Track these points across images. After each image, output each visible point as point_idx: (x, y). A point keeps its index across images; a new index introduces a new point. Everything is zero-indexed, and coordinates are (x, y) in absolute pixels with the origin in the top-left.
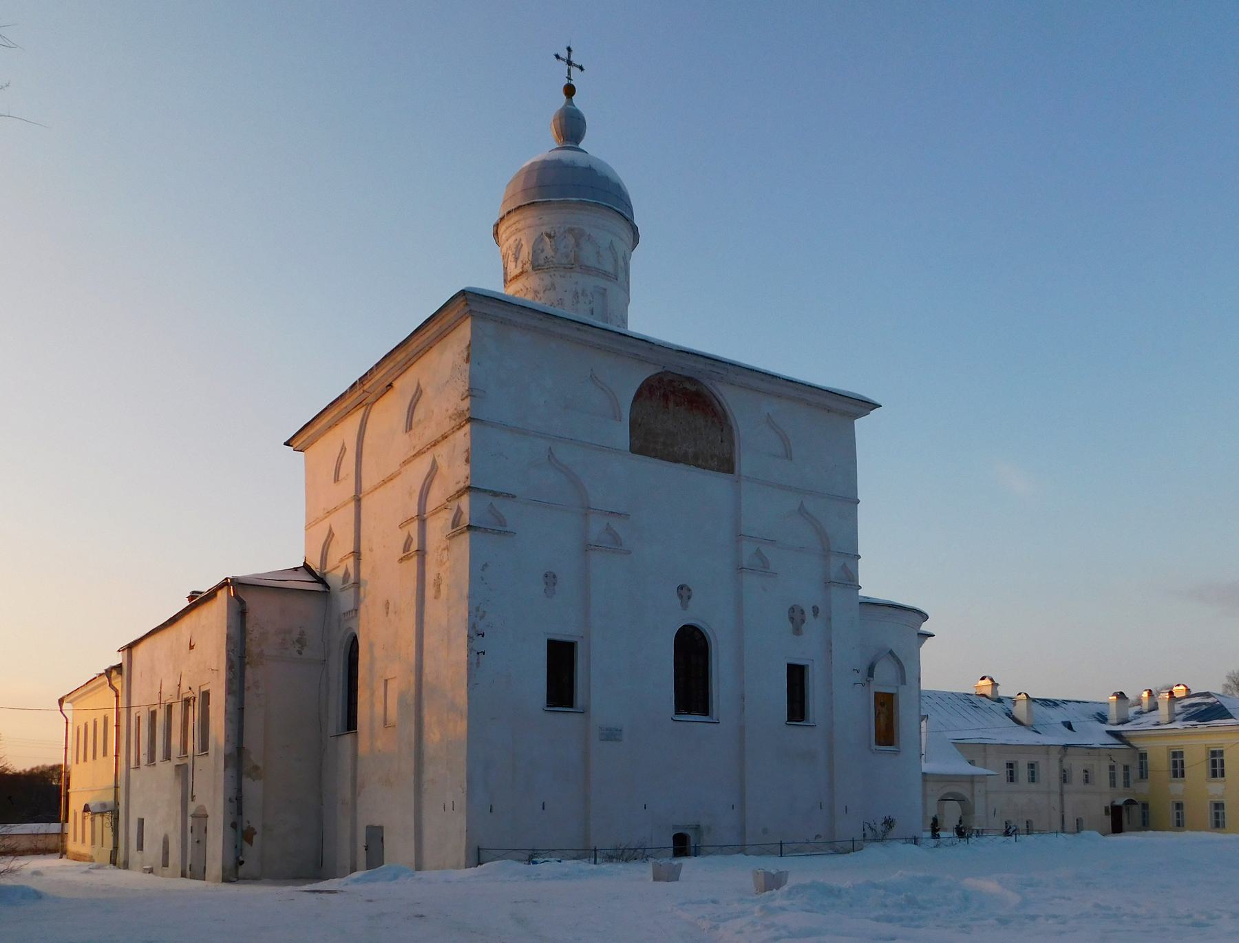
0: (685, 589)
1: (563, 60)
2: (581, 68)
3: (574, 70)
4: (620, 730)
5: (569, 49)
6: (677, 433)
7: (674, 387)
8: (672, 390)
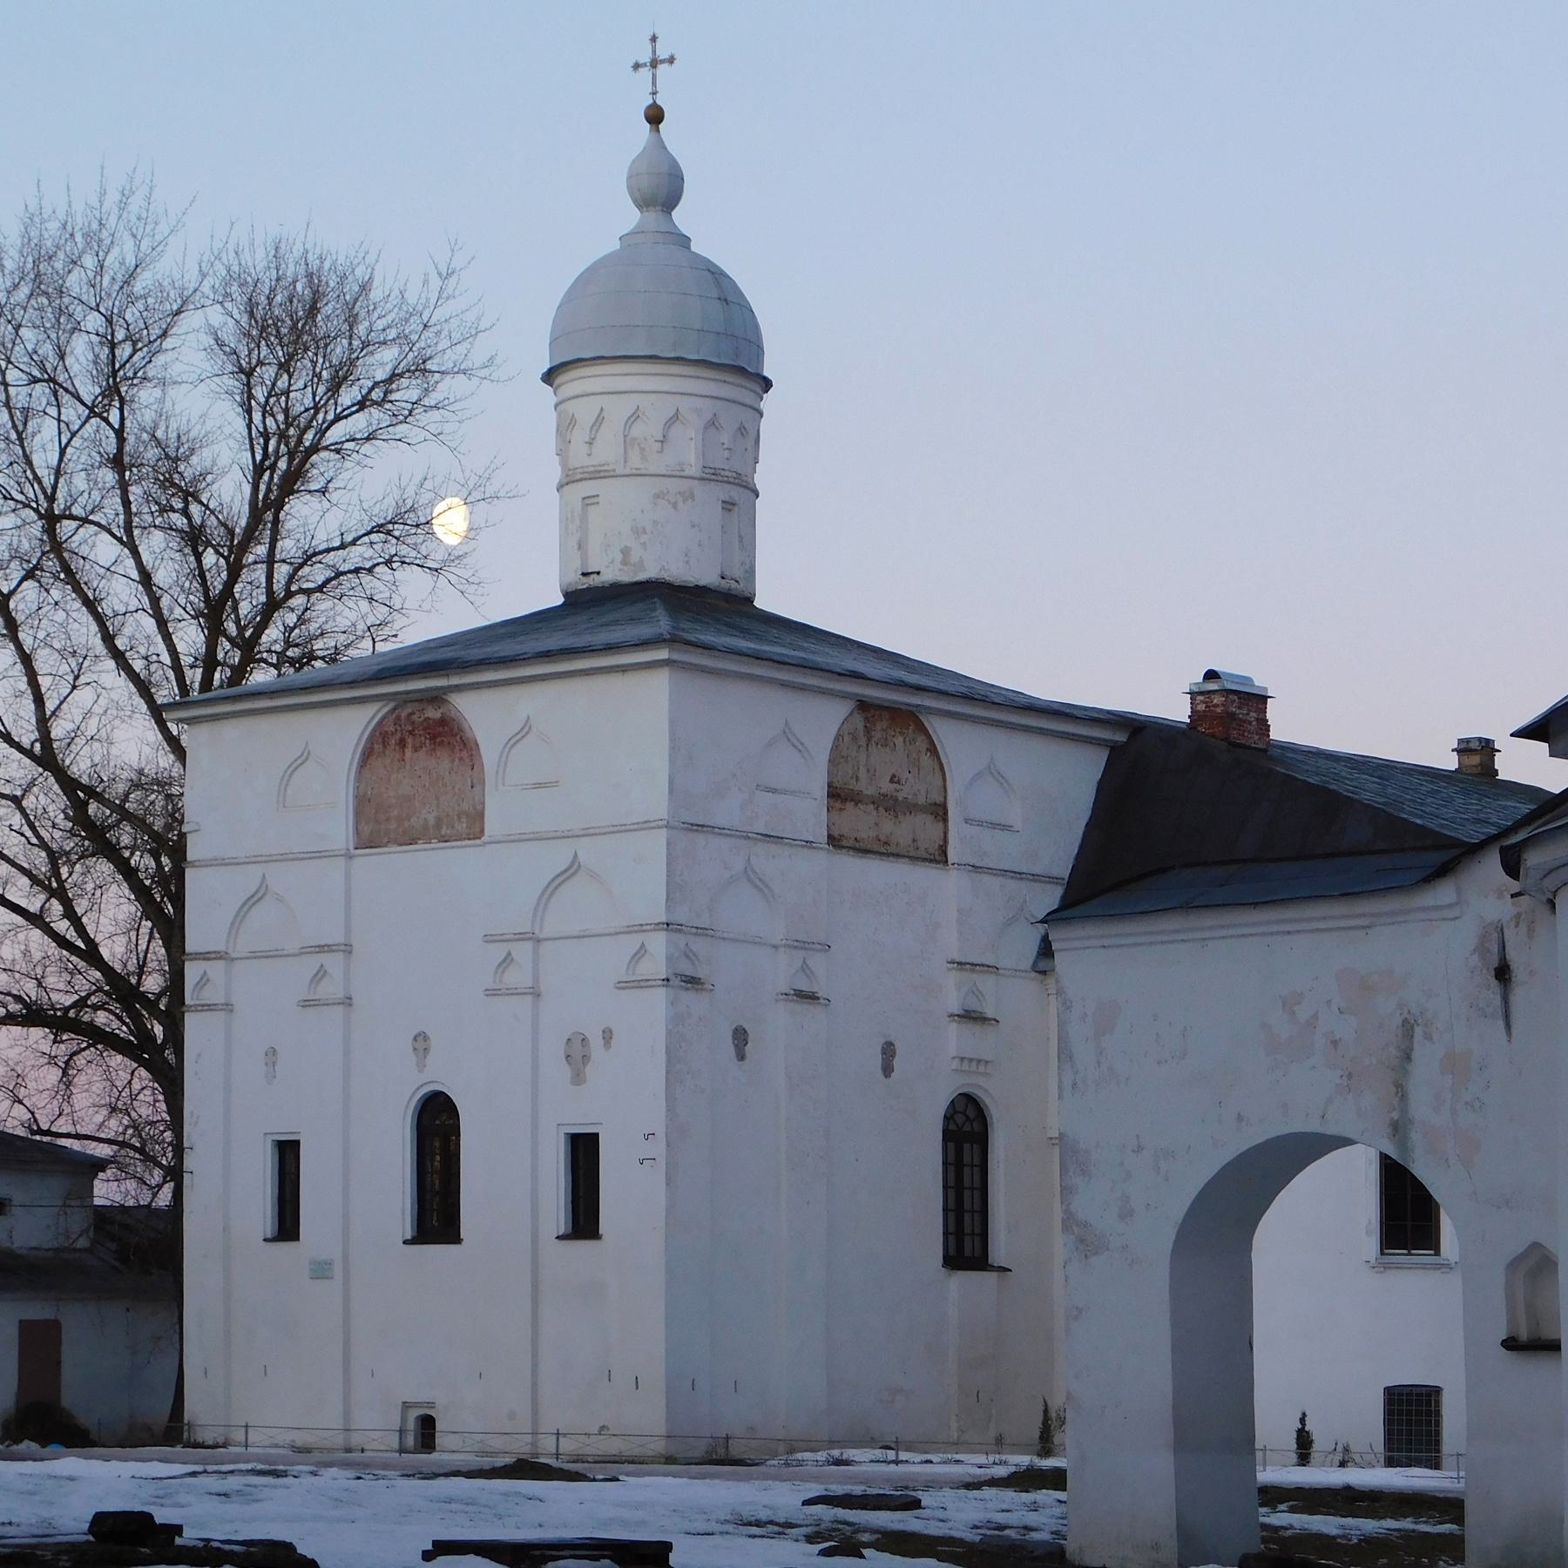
0: (420, 1039)
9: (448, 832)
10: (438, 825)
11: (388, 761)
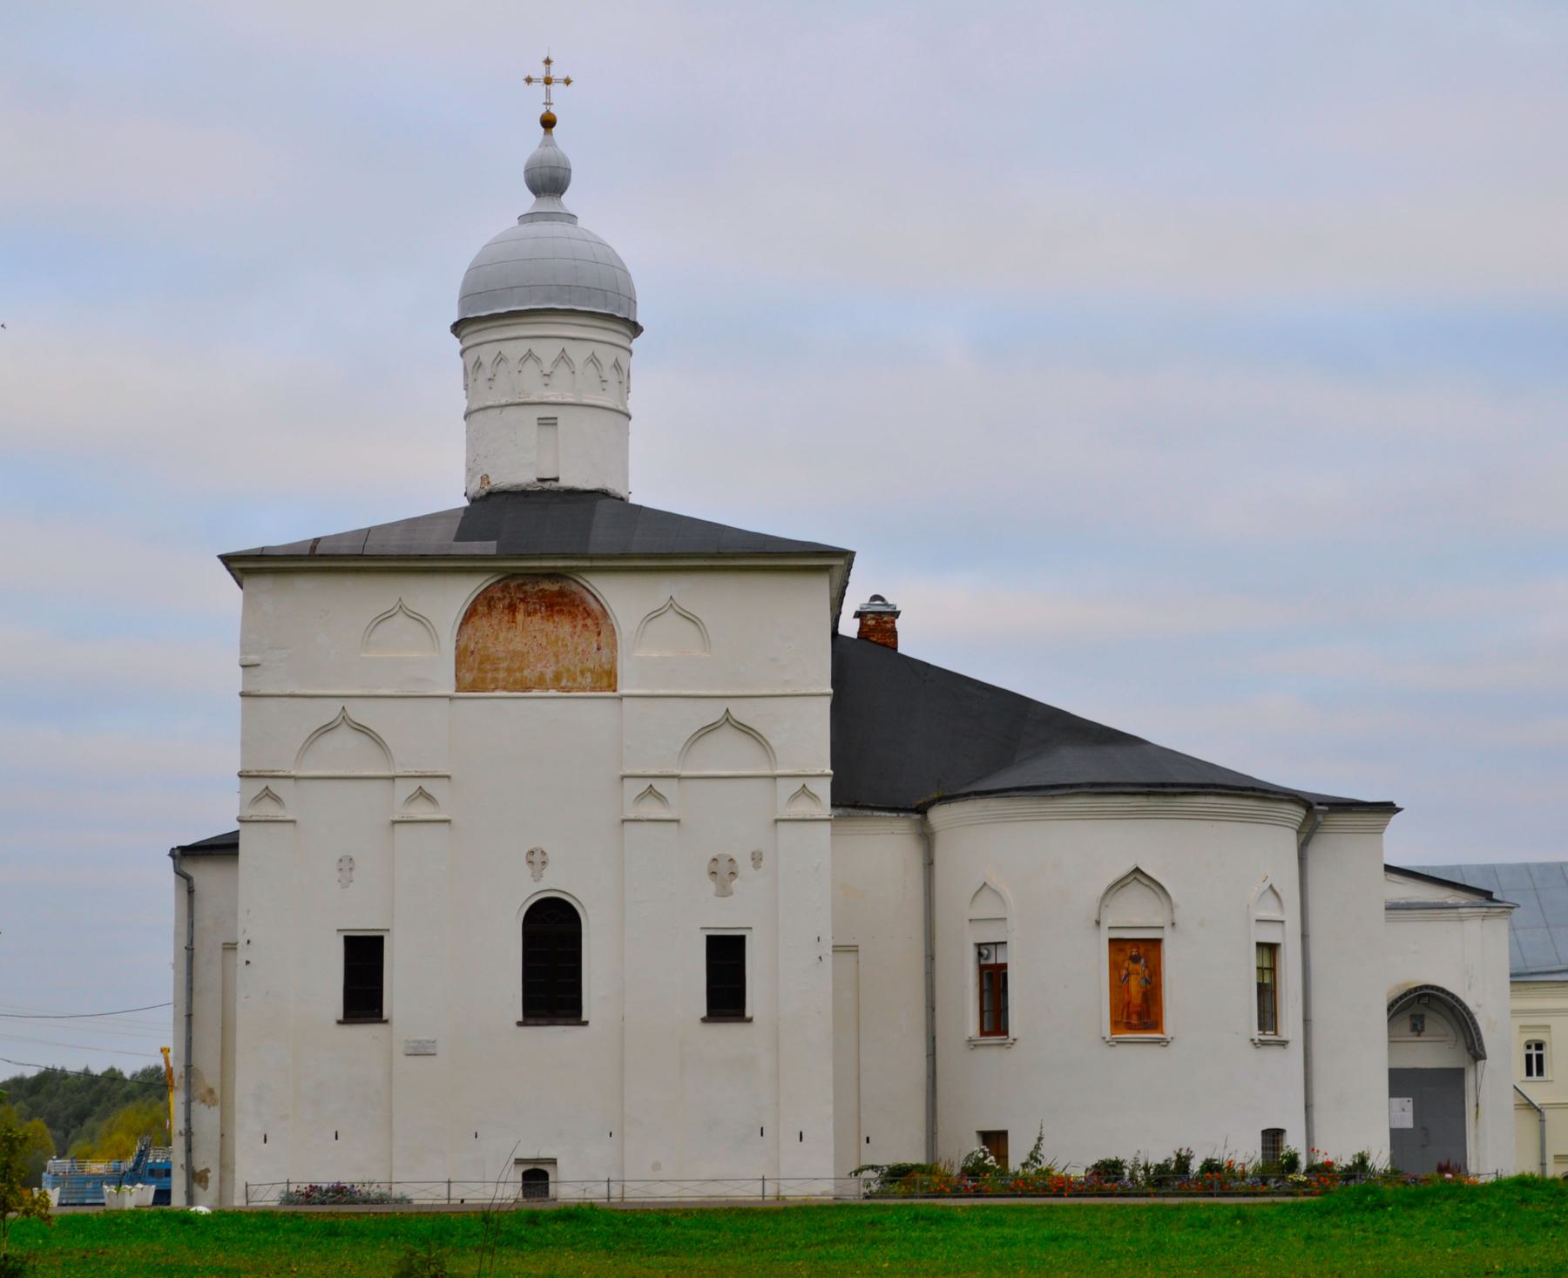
4: (433, 1042)
6: (528, 652)
7: (525, 592)
8: (522, 596)
10: (557, 677)
11: (495, 622)
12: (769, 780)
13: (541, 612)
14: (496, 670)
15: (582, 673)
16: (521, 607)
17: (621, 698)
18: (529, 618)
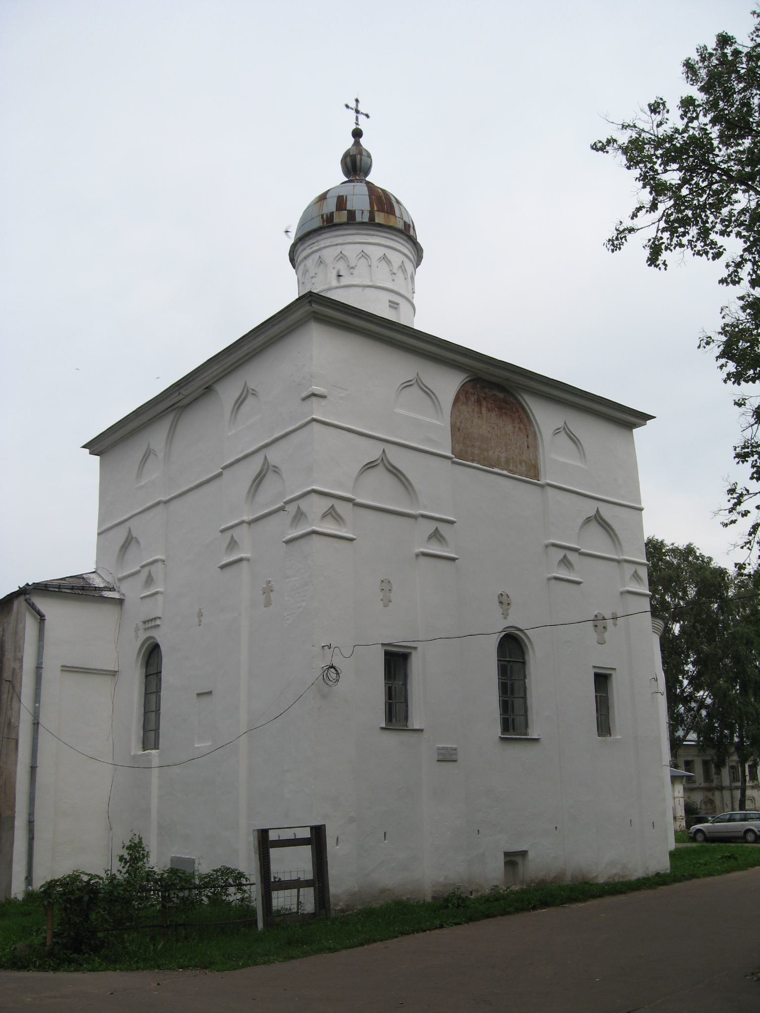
0: (505, 597)
1: (352, 109)
2: (367, 116)
3: (362, 118)
4: (456, 750)
5: (357, 101)
8: (484, 396)
9: (514, 469)
10: (507, 462)
12: (615, 564)
13: (496, 412)
14: (473, 446)
15: (521, 463)
16: (484, 403)
17: (542, 486)
18: (490, 413)
